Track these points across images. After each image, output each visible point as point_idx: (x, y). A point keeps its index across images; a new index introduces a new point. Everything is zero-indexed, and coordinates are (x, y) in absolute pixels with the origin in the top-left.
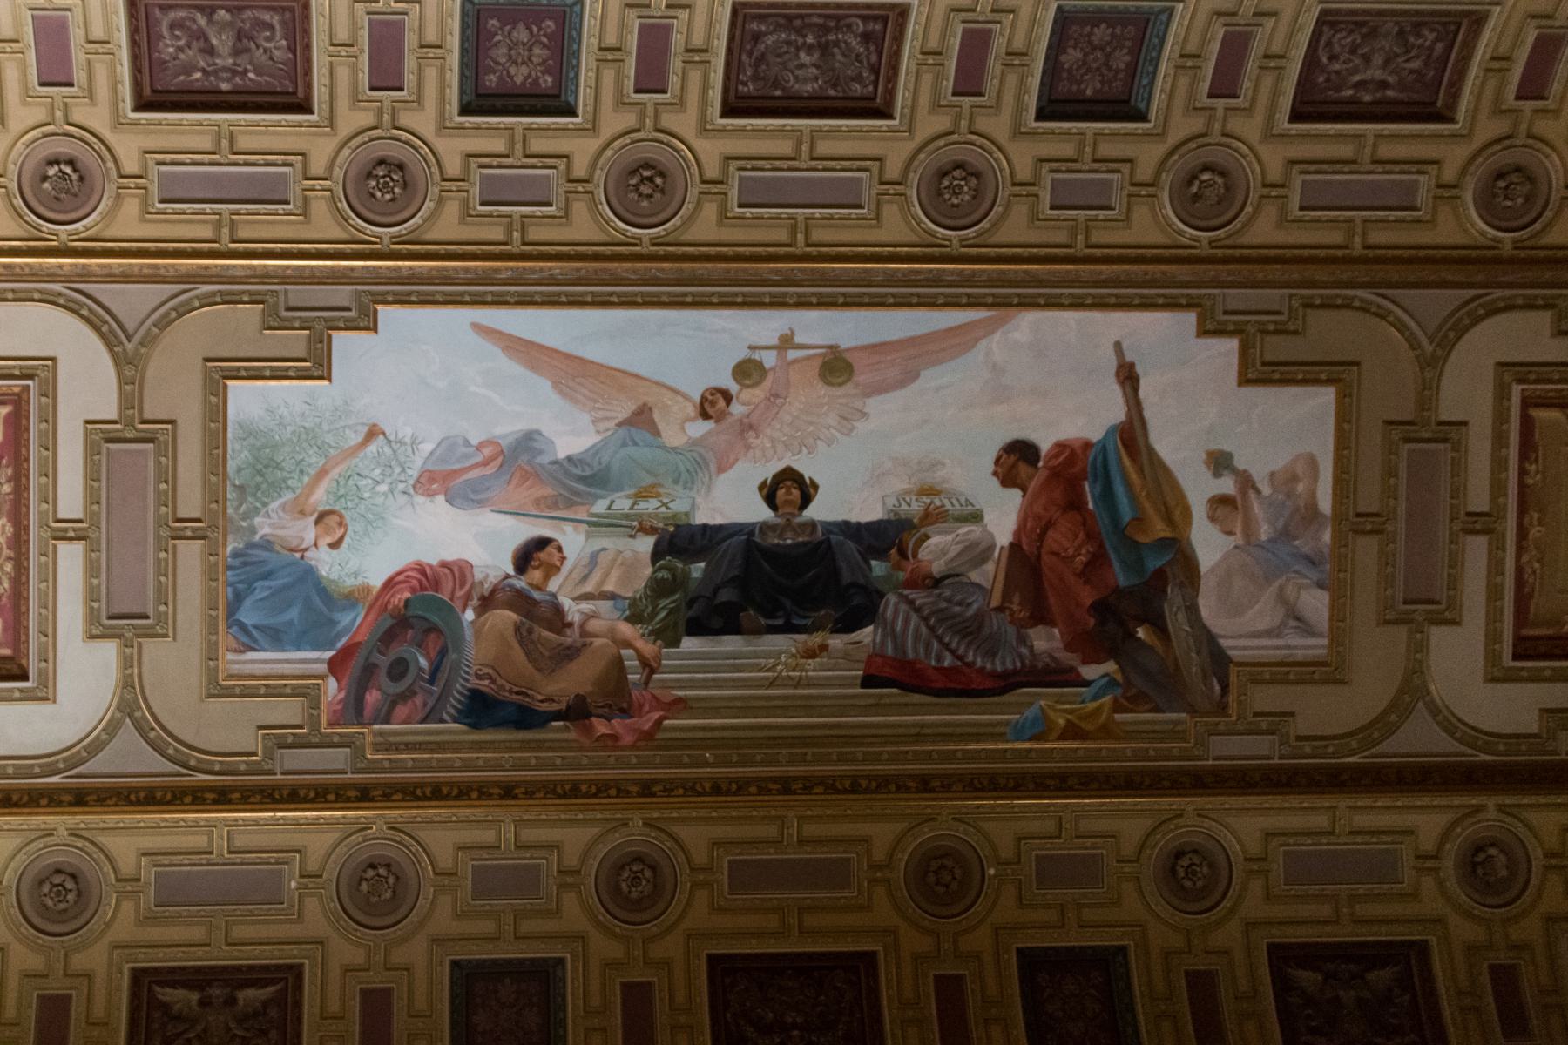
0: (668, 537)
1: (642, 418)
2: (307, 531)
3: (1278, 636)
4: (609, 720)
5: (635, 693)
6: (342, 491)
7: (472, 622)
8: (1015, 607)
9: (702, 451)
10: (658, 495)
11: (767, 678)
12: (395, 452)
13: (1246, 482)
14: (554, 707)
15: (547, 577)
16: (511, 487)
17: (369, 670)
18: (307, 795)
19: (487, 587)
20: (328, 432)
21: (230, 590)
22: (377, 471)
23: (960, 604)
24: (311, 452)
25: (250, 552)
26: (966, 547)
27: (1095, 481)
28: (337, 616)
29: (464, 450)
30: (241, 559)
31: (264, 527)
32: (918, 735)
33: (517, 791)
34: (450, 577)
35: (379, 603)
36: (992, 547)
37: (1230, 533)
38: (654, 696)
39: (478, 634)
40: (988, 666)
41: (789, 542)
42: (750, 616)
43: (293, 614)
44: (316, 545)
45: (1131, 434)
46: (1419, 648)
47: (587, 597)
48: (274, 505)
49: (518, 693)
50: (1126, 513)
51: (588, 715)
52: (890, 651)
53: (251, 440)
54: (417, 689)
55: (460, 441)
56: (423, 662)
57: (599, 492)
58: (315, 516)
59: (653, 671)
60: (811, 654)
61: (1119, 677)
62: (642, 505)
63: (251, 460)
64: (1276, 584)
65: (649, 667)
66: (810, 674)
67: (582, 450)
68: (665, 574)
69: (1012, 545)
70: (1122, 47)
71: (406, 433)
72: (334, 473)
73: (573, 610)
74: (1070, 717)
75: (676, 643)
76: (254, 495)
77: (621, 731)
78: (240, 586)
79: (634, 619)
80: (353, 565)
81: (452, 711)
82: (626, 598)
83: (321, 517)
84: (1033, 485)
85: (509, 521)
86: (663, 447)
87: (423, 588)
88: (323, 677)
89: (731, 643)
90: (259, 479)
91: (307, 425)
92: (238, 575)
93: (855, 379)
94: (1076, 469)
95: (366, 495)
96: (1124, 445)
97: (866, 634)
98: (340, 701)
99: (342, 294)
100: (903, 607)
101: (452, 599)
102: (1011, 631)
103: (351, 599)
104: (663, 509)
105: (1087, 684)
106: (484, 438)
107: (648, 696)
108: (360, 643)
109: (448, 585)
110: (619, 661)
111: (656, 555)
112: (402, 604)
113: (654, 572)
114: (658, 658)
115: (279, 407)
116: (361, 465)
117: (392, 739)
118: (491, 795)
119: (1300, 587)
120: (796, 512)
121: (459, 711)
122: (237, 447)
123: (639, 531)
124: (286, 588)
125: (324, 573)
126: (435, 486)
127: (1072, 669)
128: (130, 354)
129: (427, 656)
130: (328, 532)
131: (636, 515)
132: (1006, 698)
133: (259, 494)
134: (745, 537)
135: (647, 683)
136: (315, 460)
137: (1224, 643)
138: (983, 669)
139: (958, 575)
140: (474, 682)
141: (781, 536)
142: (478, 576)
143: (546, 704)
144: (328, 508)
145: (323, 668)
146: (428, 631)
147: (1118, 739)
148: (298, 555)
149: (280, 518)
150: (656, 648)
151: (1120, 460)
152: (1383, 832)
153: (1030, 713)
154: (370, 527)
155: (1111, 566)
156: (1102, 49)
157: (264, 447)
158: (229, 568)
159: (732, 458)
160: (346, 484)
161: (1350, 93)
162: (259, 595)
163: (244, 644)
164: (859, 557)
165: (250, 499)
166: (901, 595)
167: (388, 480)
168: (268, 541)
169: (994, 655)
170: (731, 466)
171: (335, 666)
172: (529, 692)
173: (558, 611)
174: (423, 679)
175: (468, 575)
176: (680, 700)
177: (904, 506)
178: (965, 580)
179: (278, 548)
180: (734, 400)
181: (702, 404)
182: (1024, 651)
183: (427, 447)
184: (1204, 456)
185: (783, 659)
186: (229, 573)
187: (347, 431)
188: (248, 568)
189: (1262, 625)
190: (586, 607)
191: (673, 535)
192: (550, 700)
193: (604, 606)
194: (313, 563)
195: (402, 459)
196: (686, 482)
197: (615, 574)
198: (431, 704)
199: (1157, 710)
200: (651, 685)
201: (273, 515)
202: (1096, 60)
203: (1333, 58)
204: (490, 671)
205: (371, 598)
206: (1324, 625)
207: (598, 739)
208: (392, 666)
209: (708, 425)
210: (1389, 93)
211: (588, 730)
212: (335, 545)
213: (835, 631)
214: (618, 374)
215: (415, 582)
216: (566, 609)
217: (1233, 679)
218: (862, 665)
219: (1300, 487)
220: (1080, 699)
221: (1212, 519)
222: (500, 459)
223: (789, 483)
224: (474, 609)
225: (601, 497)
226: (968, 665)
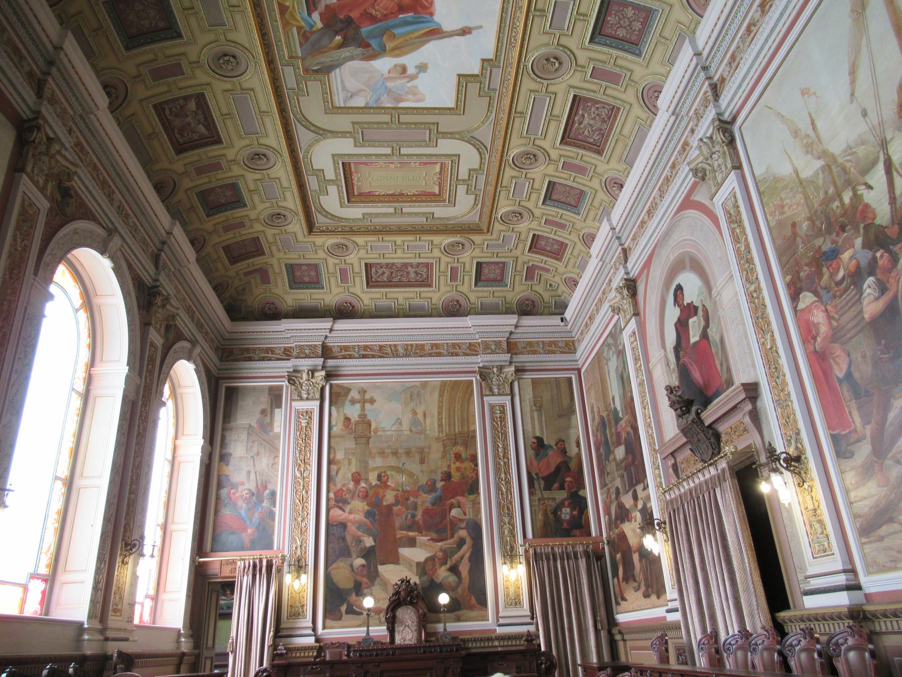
3: (343, 90)
13: (413, 78)
27: (413, 17)
37: (389, 72)
45: (436, 33)
46: (343, 134)
50: (397, 31)
61: (315, 29)
64: (366, 89)
70: (627, 34)
94: (419, 9)
96: (431, 31)
105: (309, 15)
119: (366, 97)
127: (316, 9)
137: (337, 70)
151: (423, 29)
155: (370, 25)
156: (629, 25)
189: (347, 84)
202: (625, 22)
203: (597, 108)
206: (349, 105)
217: (320, 77)
219: (410, 96)
220: (301, 12)
221: (396, 66)
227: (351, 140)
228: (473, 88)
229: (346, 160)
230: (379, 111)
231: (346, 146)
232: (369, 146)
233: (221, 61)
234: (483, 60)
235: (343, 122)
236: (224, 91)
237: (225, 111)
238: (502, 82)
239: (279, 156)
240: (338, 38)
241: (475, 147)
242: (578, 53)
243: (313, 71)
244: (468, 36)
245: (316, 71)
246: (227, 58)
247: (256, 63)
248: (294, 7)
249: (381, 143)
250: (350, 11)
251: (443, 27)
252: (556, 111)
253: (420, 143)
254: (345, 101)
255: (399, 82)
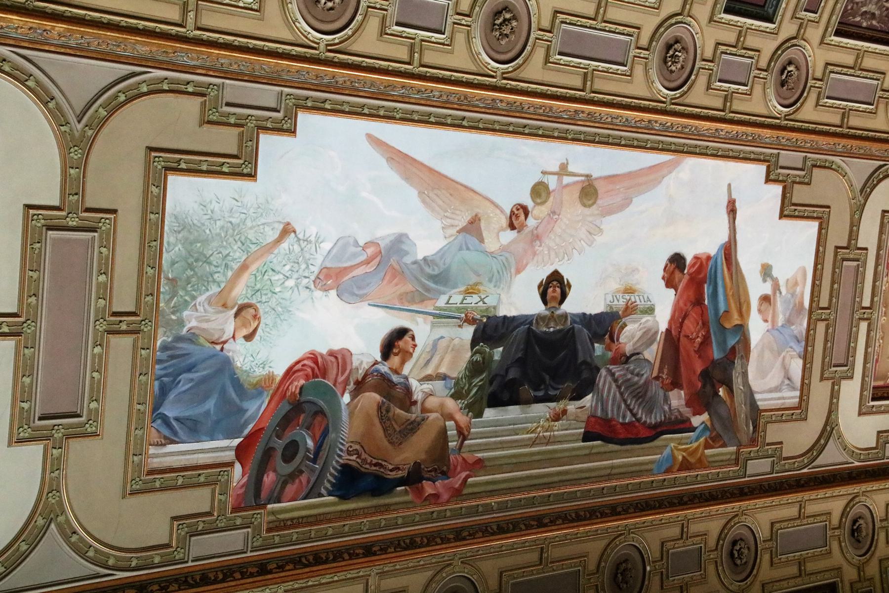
0: (482, 327)
1: (473, 227)
2: (227, 324)
4: (434, 482)
5: (452, 457)
6: (258, 286)
7: (348, 404)
8: (664, 376)
9: (507, 255)
10: (478, 292)
11: (530, 439)
12: (302, 250)
13: (776, 287)
14: (400, 474)
15: (403, 362)
16: (385, 282)
17: (268, 453)
18: (216, 577)
19: (360, 374)
20: (251, 228)
21: (157, 383)
22: (288, 267)
23: (638, 375)
24: (235, 247)
25: (180, 345)
26: (645, 332)
28: (245, 405)
29: (353, 249)
30: (169, 353)
31: (191, 320)
32: (609, 475)
33: (374, 549)
34: (335, 364)
35: (281, 389)
36: (656, 332)
37: (766, 321)
38: (464, 459)
39: (351, 414)
40: (648, 421)
41: (552, 330)
42: (526, 390)
43: (210, 405)
44: (234, 337)
45: (729, 251)
46: (834, 395)
47: (428, 378)
48: (201, 299)
49: (376, 465)
50: (722, 307)
51: (420, 479)
52: (599, 413)
53: (184, 234)
54: (303, 469)
55: (351, 241)
56: (310, 443)
57: (442, 288)
58: (235, 309)
59: (465, 439)
60: (557, 417)
61: (709, 424)
62: (469, 300)
63: (184, 252)
65: (463, 435)
66: (556, 433)
67: (434, 252)
68: (478, 357)
69: (667, 330)
71: (312, 231)
72: (253, 268)
73: (418, 389)
74: (684, 454)
75: (479, 414)
76: (184, 289)
77: (441, 490)
78: (165, 379)
79: (456, 396)
80: (261, 357)
81: (328, 486)
82: (453, 379)
83: (242, 309)
84: (681, 287)
85: (380, 313)
86: (485, 252)
87: (315, 376)
88: (231, 464)
89: (513, 412)
90: (190, 273)
91: (233, 220)
92: (165, 368)
93: (599, 202)
94: (701, 276)
95: (277, 290)
96: (725, 258)
97: (588, 400)
98: (242, 486)
99: (267, 94)
100: (609, 379)
101: (335, 385)
102: (661, 393)
103: (259, 388)
104: (481, 304)
105: (693, 429)
106: (368, 239)
107: (460, 459)
108: (263, 429)
109: (332, 372)
110: (444, 431)
111: (474, 342)
112: (298, 391)
113: (472, 356)
114: (469, 428)
115: (211, 202)
116: (275, 261)
117: (282, 516)
118: (358, 555)
120: (557, 306)
121: (333, 485)
122: (172, 240)
123: (465, 321)
124: (204, 380)
125: (239, 365)
126: (329, 282)
128: (77, 134)
129: (313, 438)
130: (244, 325)
131: (463, 308)
132: (657, 443)
133: (189, 288)
134: (527, 326)
135: (460, 449)
136: (238, 256)
138: (645, 422)
139: (638, 354)
140: (346, 458)
141: (547, 326)
142: (355, 363)
143: (394, 473)
144: (246, 301)
145: (230, 455)
146: (316, 413)
147: (705, 468)
148: (218, 347)
149: (205, 311)
150: (468, 419)
152: (819, 515)
153: (667, 452)
154: (279, 321)
155: (712, 346)
157: (196, 241)
158: (159, 361)
159: (525, 262)
160: (262, 279)
161: (858, 19)
162: (182, 387)
163: (165, 438)
164: (588, 340)
165: (181, 293)
166: (609, 371)
167: (295, 276)
168: (194, 334)
169: (651, 412)
170: (524, 269)
171: (241, 452)
172: (384, 463)
173: (408, 391)
174: (308, 459)
175: (348, 361)
176: (480, 461)
177: (616, 302)
178: (641, 356)
179: (202, 340)
180: (530, 215)
181: (511, 217)
182: (666, 408)
183: (326, 246)
184: (759, 268)
185: (542, 423)
186: (157, 367)
187: (267, 229)
188: (174, 361)
190: (427, 386)
191: (485, 325)
192: (397, 469)
193: (439, 385)
194: (230, 354)
195: (307, 256)
196: (496, 282)
197: (448, 358)
198: (313, 479)
199: (724, 445)
200: (463, 450)
201: (200, 309)
204: (357, 447)
205: (274, 386)
206: (798, 384)
207: (426, 499)
208: (286, 448)
209: (511, 235)
210: (874, 22)
211: (420, 492)
212: (249, 338)
213: (571, 399)
214: (462, 188)
215: (309, 370)
216: (414, 389)
218: (583, 425)
219: (798, 289)
220: (689, 441)
221: (760, 311)
222: (378, 259)
223: (555, 283)
224: (350, 392)
225: (444, 294)
226: (638, 420)
227: (844, 383)
228: (800, 194)
229: (868, 394)
230: (810, 338)
231: (851, 391)
232: (854, 356)
233: (739, 562)
234: (768, 180)
235: (820, 392)
236: (772, 565)
237: (794, 570)
238: (797, 149)
239: (857, 500)
240: (721, 392)
241: (875, 186)
242: (783, 36)
243: (754, 431)
244: (737, 204)
245: (755, 427)
246: (736, 553)
247: (743, 514)
248: (685, 450)
249: (852, 337)
250: (694, 373)
251: (724, 242)
252: (849, 60)
253: (859, 274)
254: (794, 389)
255: (780, 305)
